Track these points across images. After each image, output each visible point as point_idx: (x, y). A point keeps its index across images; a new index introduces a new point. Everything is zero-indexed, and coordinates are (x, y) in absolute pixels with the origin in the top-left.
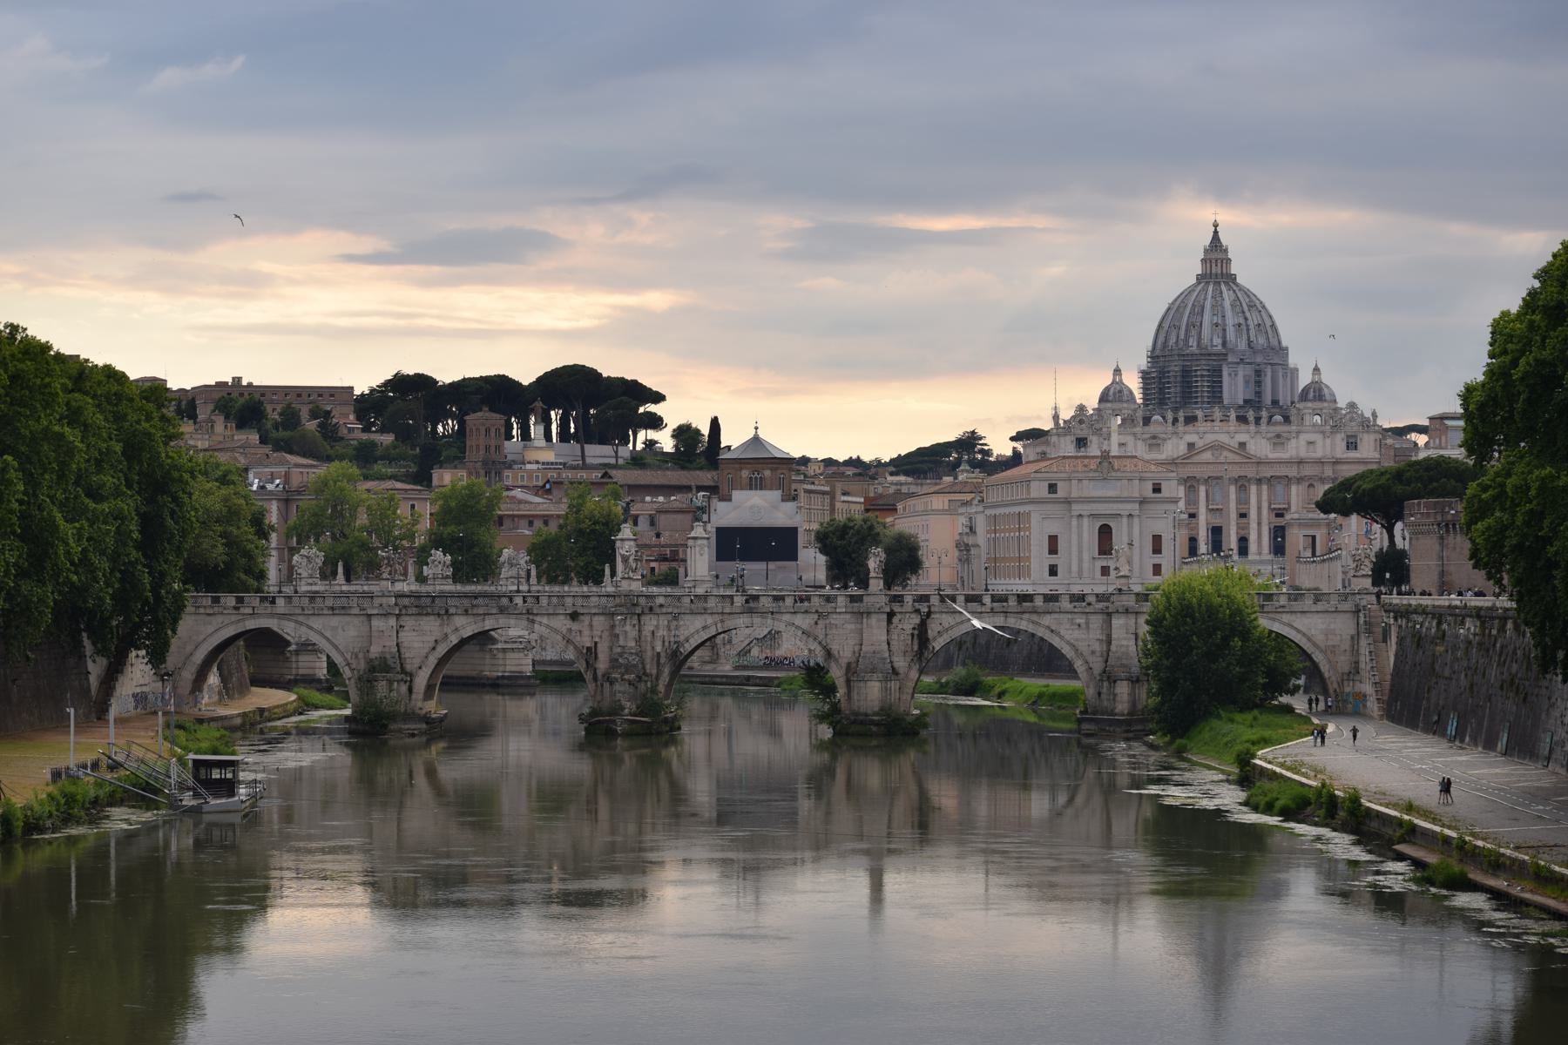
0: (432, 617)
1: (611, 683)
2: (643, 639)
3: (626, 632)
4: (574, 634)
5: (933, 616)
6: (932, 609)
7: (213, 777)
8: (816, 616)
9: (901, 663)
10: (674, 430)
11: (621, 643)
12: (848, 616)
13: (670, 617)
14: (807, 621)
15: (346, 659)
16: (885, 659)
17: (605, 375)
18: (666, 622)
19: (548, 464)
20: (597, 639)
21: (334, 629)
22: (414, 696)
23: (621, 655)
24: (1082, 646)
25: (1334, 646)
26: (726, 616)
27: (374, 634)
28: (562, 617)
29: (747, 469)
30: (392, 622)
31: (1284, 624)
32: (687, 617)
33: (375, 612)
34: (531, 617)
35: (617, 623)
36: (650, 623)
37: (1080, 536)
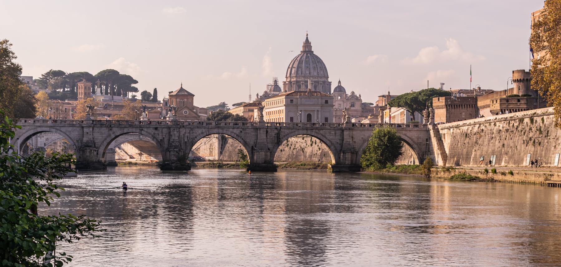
1: (170, 152)
3: (175, 134)
4: (156, 135)
10: (142, 92)
12: (252, 130)
14: (238, 131)
15: (74, 143)
18: (189, 131)
21: (70, 132)
22: (98, 156)
23: (173, 142)
25: (421, 143)
27: (84, 134)
29: (179, 98)
32: (196, 129)
33: (85, 126)
35: (172, 131)
36: (183, 131)
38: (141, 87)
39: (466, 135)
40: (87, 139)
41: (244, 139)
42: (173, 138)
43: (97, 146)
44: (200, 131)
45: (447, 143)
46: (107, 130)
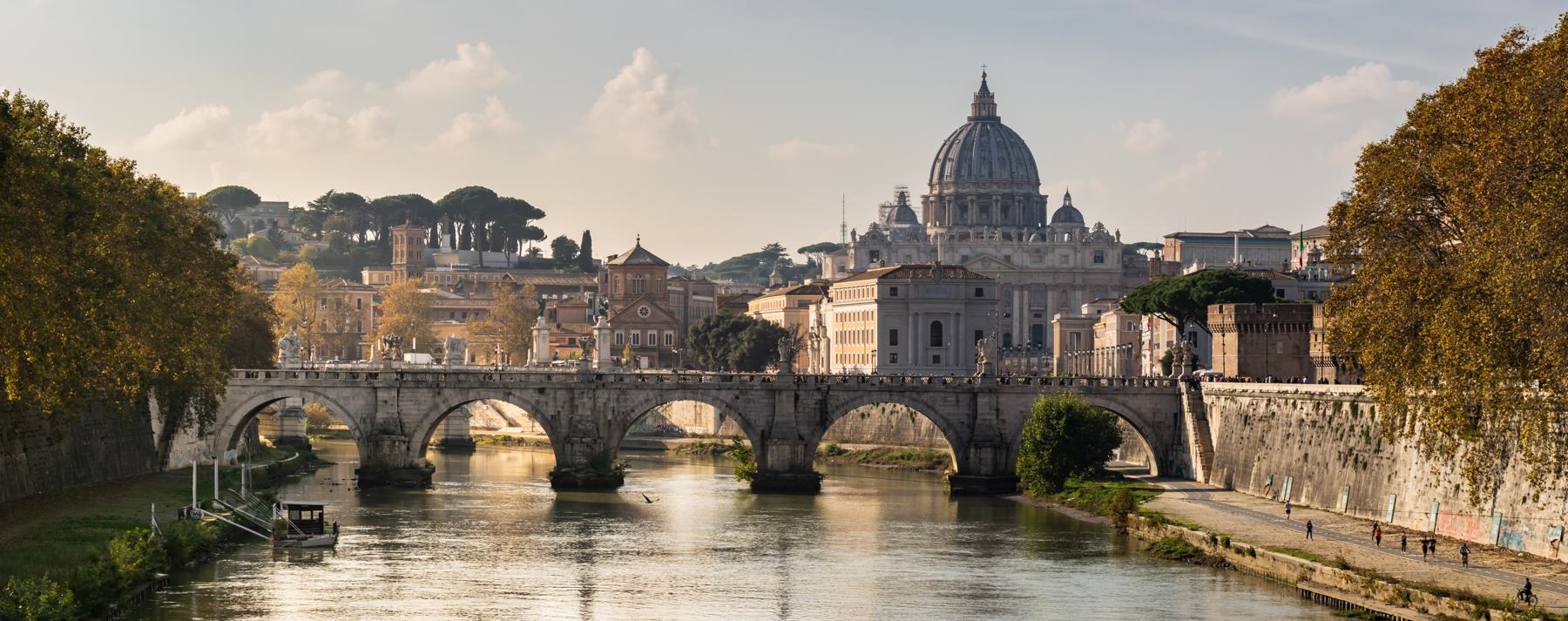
1: (572, 445)
2: (597, 408)
3: (584, 403)
4: (541, 404)
7: (303, 518)
10: (554, 241)
12: (763, 393)
14: (730, 397)
15: (356, 423)
18: (615, 396)
20: (560, 409)
21: (346, 398)
22: (411, 453)
23: (580, 422)
29: (631, 273)
32: (633, 392)
33: (380, 385)
35: (577, 396)
36: (602, 396)
38: (553, 228)
39: (1246, 417)
40: (385, 416)
41: (743, 414)
42: (580, 411)
43: (407, 430)
44: (642, 396)
45: (1215, 424)
46: (431, 395)
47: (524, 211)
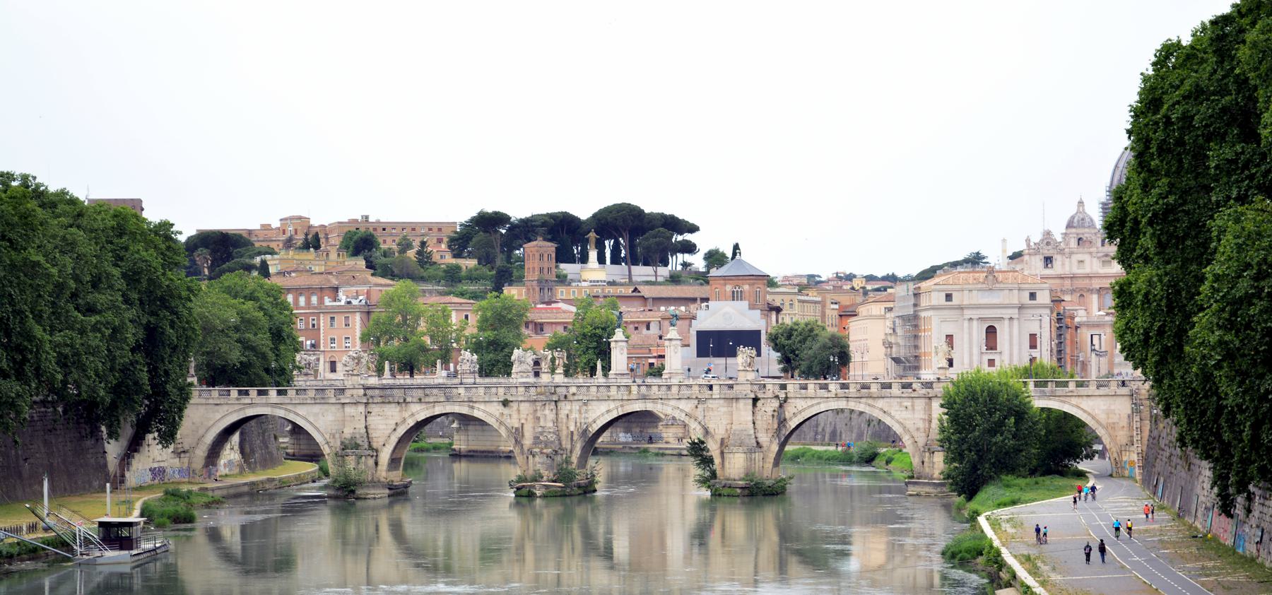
0: (393, 405)
1: (534, 456)
2: (559, 420)
3: (545, 415)
5: (789, 401)
6: (789, 396)
8: (696, 402)
9: (764, 438)
10: (706, 254)
11: (542, 423)
12: (722, 401)
13: (580, 403)
14: (689, 406)
16: (751, 435)
17: (646, 211)
18: (578, 408)
19: (594, 281)
20: (523, 421)
21: (316, 415)
22: (379, 468)
23: (541, 433)
24: (909, 424)
25: (1114, 423)
26: (625, 402)
28: (495, 404)
30: (361, 408)
31: (1073, 405)
33: (347, 401)
34: (471, 404)
35: (538, 408)
36: (565, 408)
37: (970, 334)
47: (674, 224)
